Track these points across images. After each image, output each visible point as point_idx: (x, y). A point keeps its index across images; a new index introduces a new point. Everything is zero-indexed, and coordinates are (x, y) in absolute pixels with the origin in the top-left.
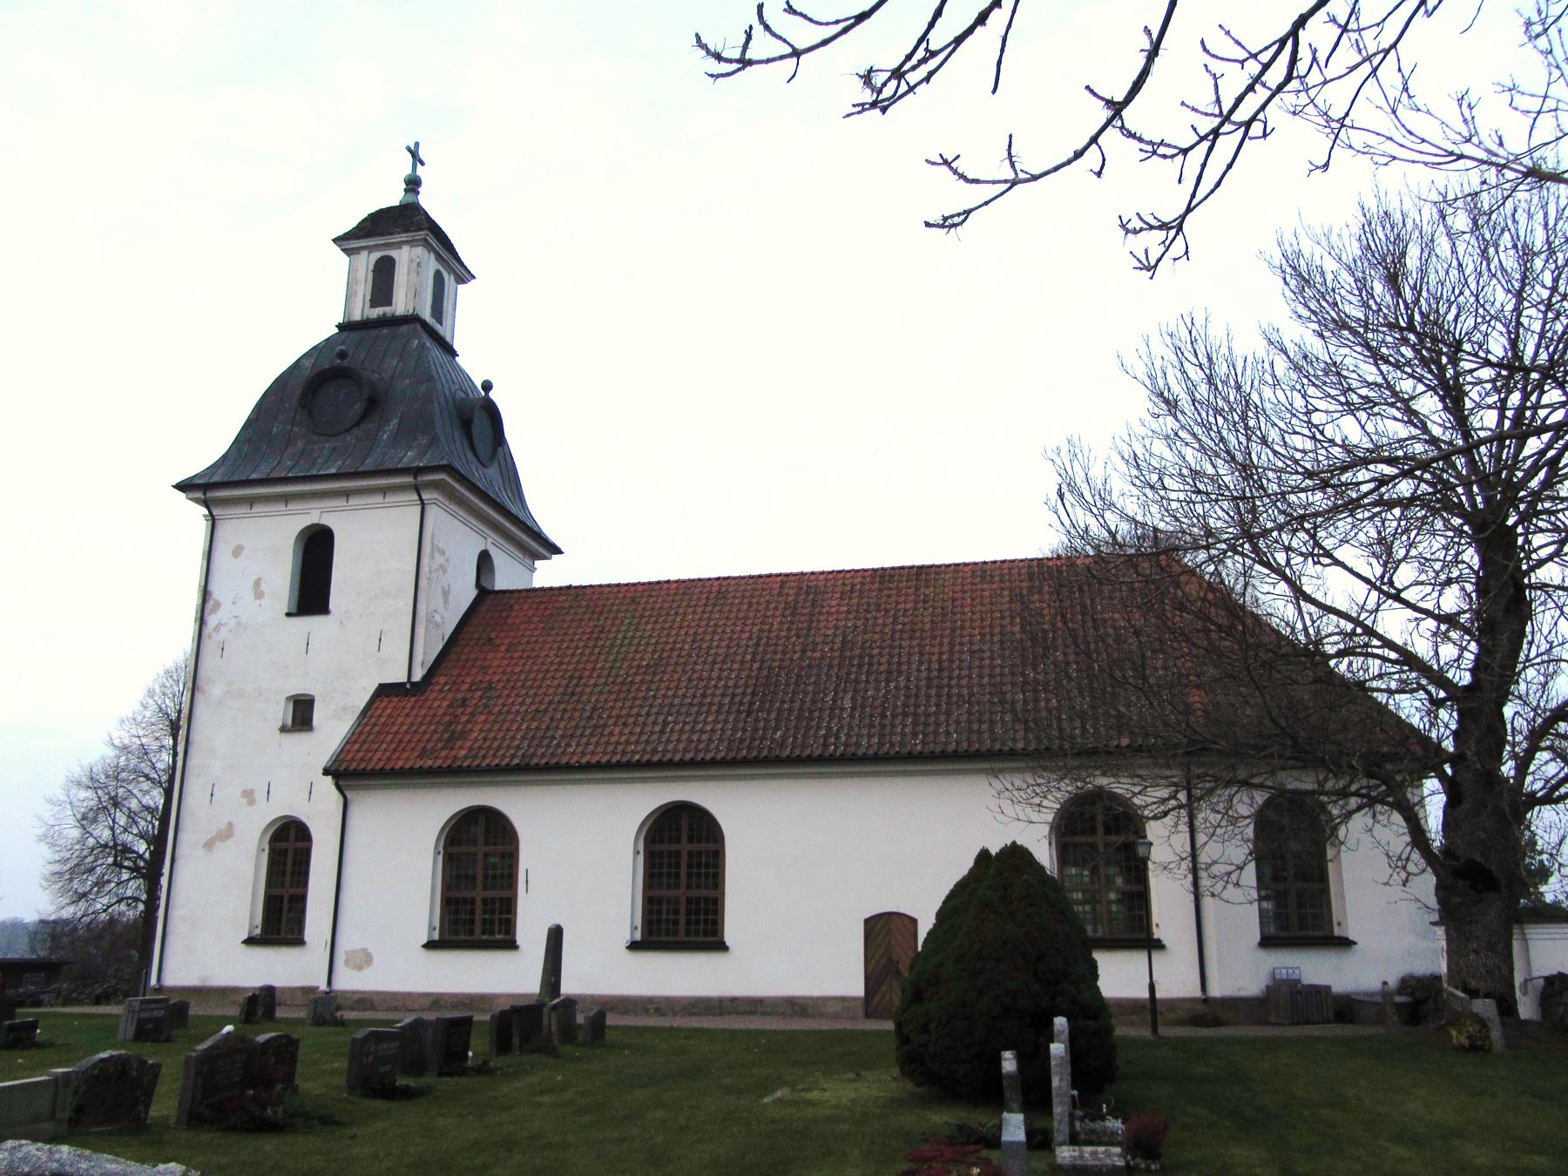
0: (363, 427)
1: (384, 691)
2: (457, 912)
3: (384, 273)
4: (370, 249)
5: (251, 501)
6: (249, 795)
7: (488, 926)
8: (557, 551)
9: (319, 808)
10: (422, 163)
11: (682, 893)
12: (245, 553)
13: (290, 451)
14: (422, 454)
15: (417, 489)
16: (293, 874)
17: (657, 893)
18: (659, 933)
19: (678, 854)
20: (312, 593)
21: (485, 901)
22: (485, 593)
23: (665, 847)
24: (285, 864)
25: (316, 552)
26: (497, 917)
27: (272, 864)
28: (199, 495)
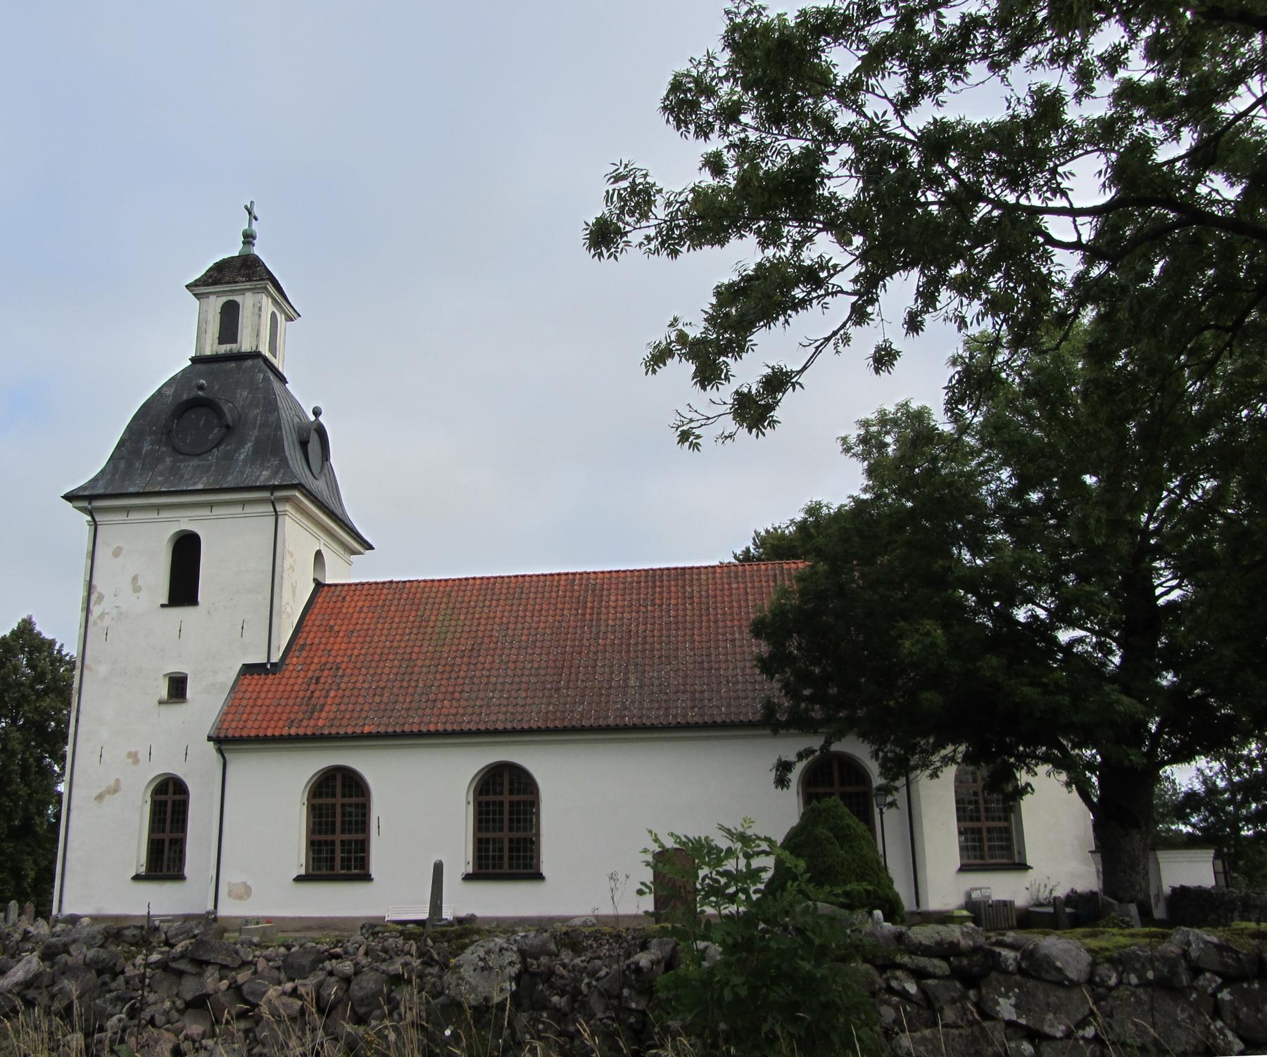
1: (249, 670)
2: (320, 852)
3: (230, 314)
4: (218, 294)
5: (127, 510)
6: (134, 757)
7: (346, 863)
8: (370, 547)
9: (199, 770)
10: (256, 219)
11: (505, 835)
13: (160, 467)
14: (275, 474)
16: (172, 821)
17: (484, 835)
18: (487, 867)
19: (501, 804)
20: (183, 588)
21: (343, 842)
22: (319, 585)
23: (491, 798)
24: (165, 813)
25: (186, 552)
26: (353, 855)
27: (154, 813)
28: (85, 504)
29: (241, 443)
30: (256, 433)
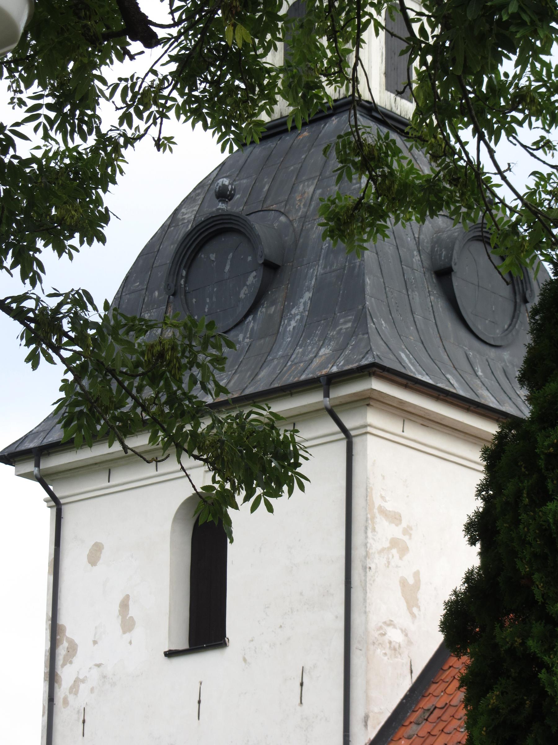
0: (262, 312)
12: (105, 554)
15: (333, 414)
28: (30, 467)
29: (292, 299)
30: (319, 270)
